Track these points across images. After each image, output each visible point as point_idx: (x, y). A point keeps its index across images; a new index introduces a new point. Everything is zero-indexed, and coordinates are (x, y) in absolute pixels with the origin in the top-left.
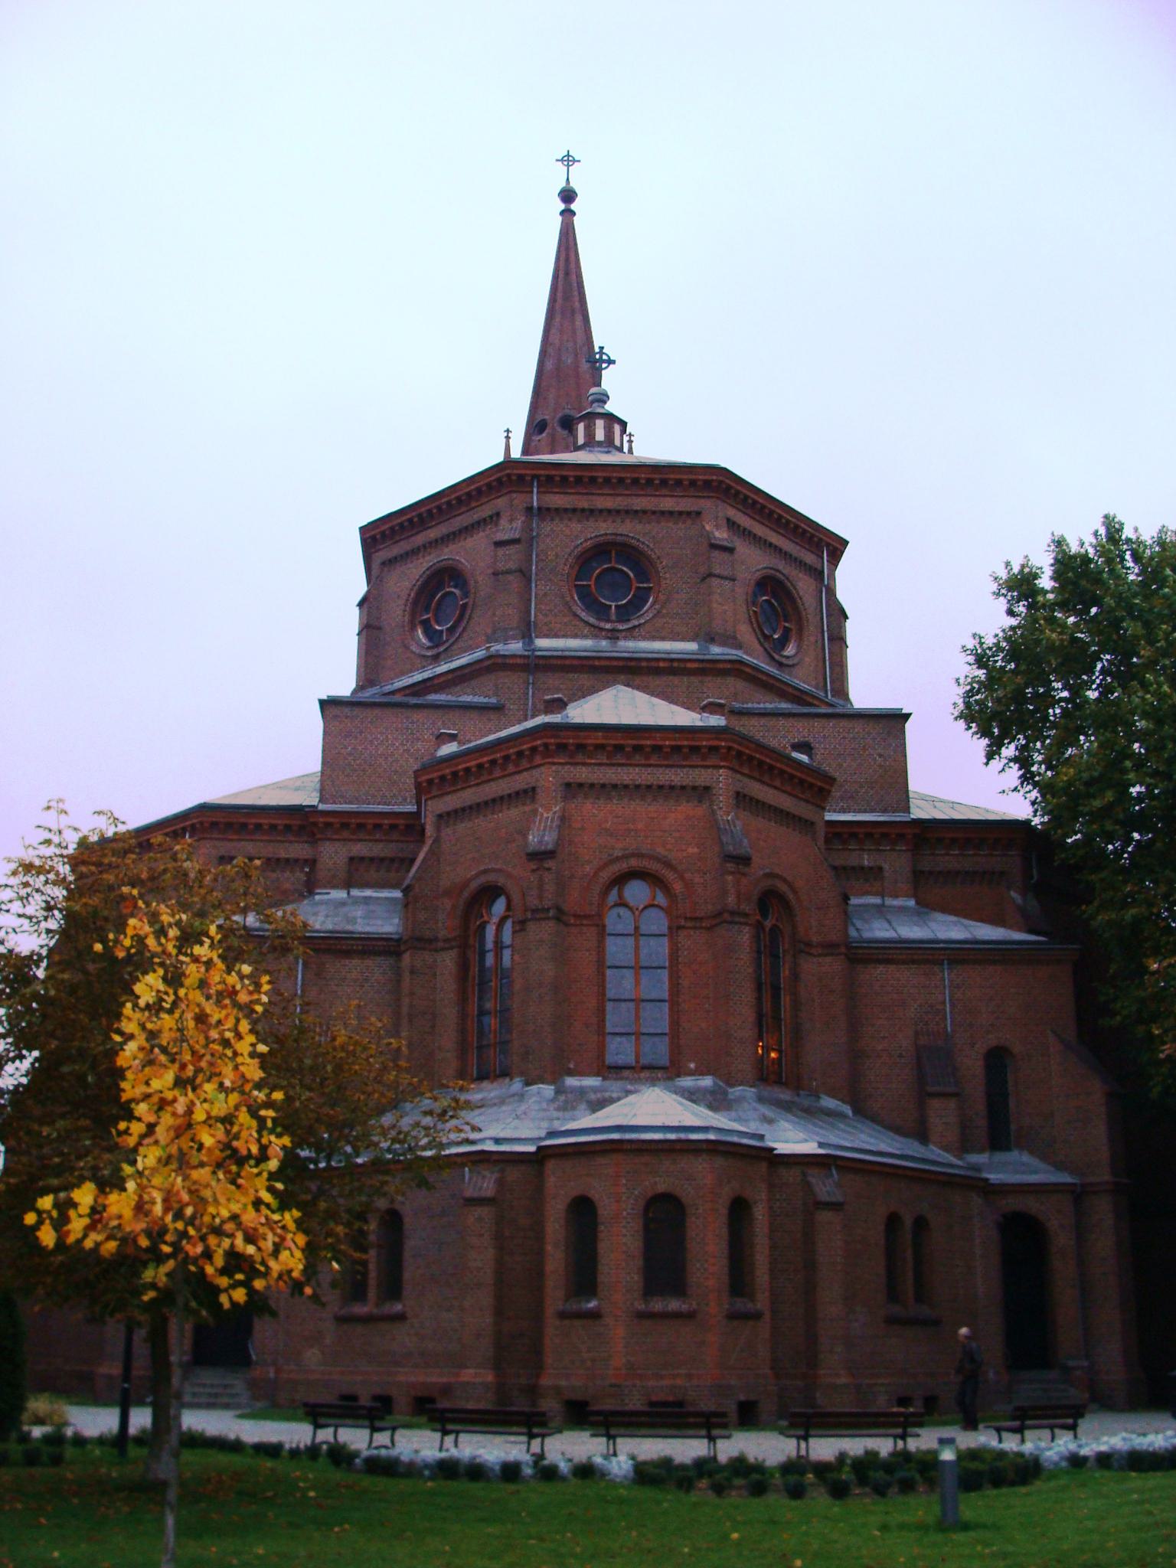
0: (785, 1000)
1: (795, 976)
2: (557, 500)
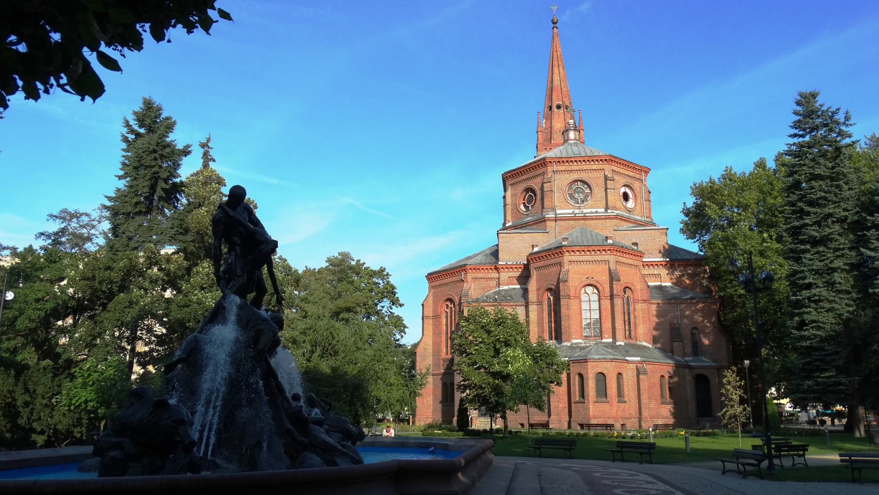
0: (632, 316)
1: (635, 310)
2: (561, 168)
